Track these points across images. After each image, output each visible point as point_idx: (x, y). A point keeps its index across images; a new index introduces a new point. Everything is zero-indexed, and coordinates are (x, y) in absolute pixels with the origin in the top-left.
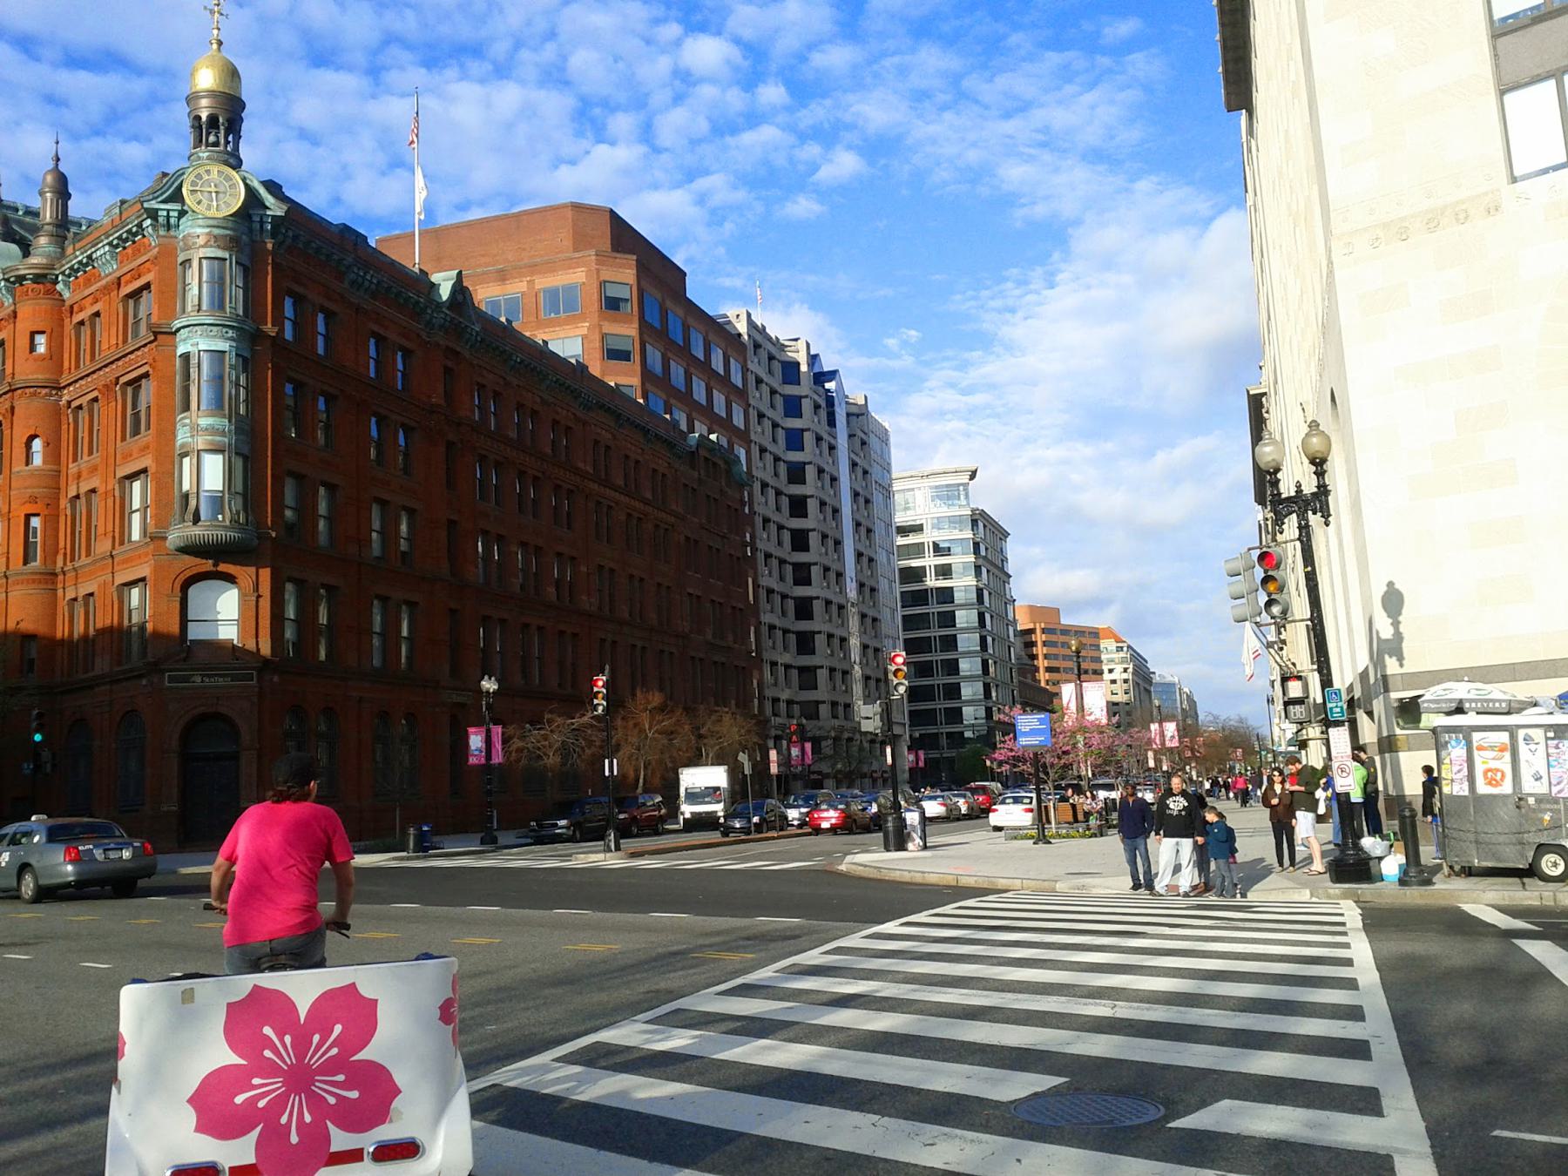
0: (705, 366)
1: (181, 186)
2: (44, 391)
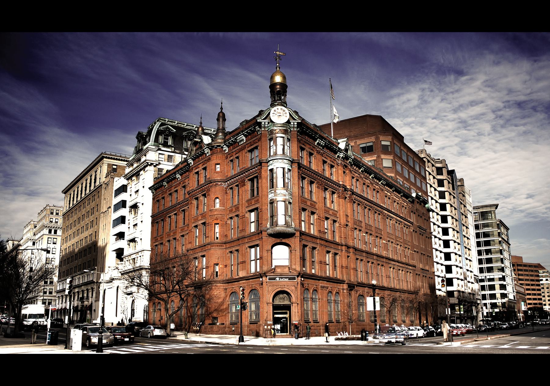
0: (414, 169)
1: (269, 114)
2: (219, 183)
